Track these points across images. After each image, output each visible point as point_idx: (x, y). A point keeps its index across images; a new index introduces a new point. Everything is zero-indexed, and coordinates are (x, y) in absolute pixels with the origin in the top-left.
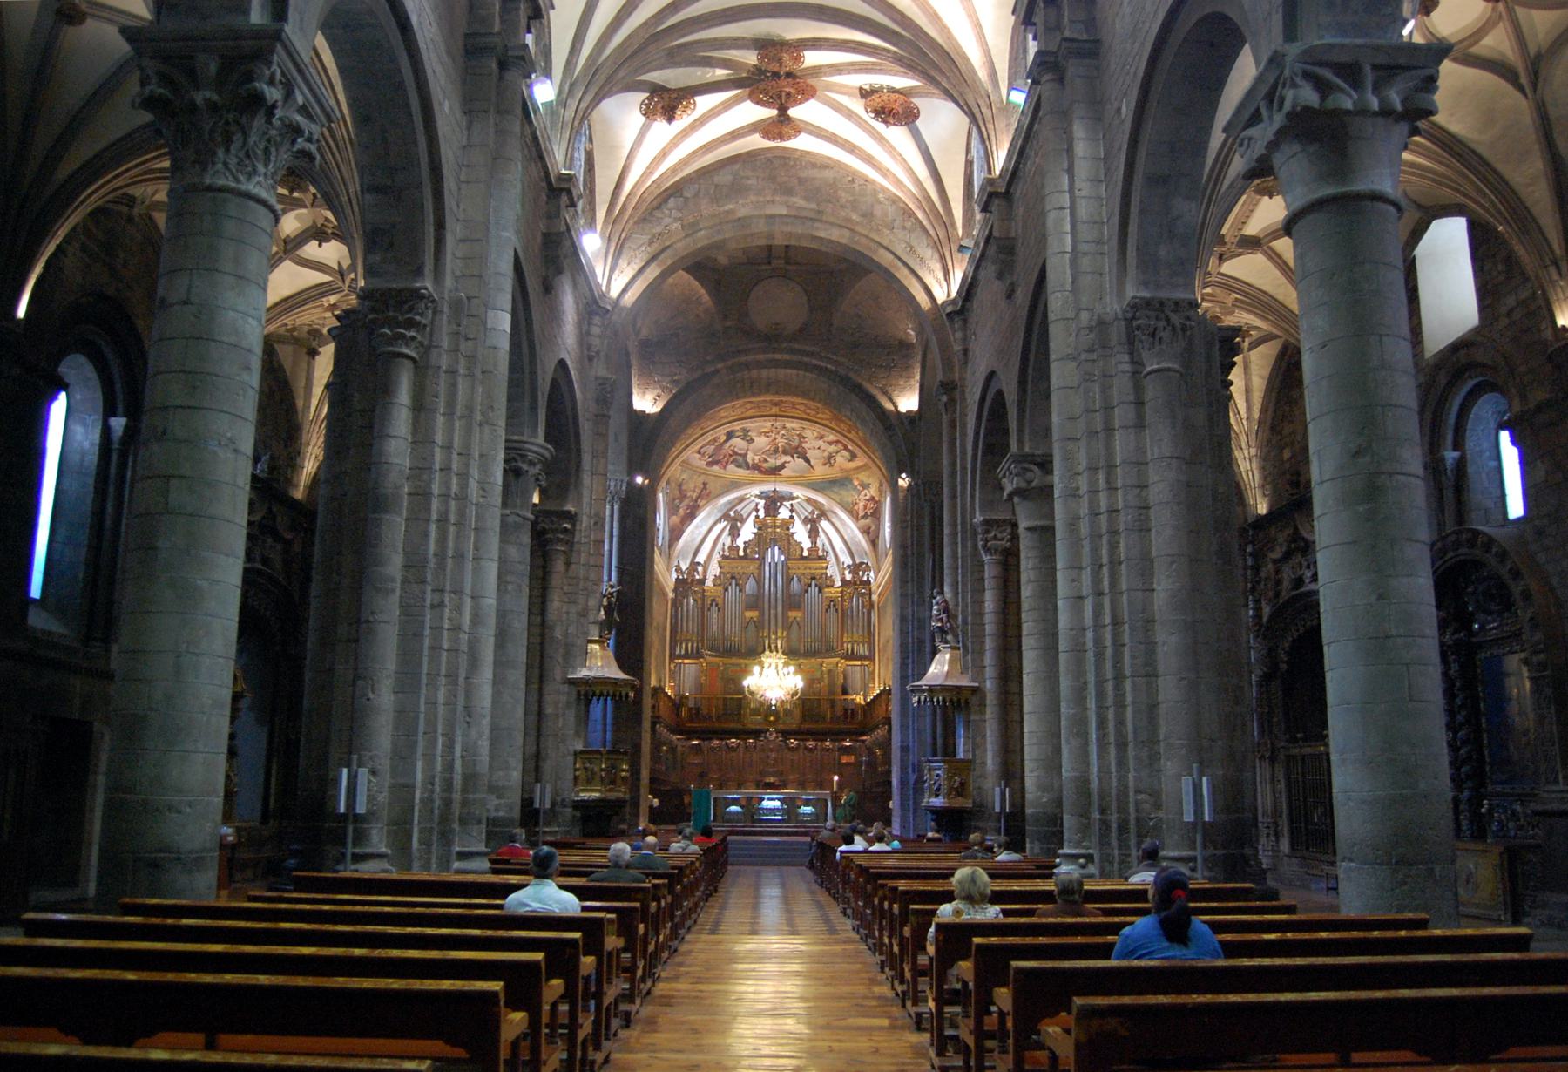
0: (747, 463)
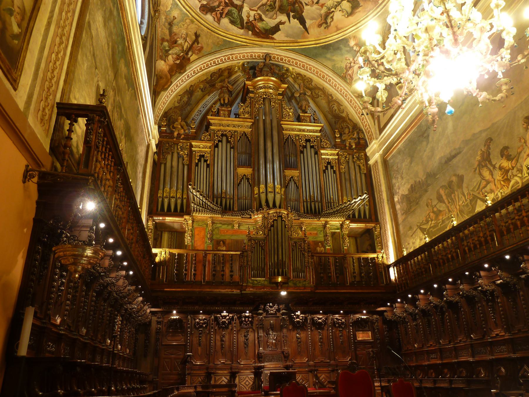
0: (242, 19)
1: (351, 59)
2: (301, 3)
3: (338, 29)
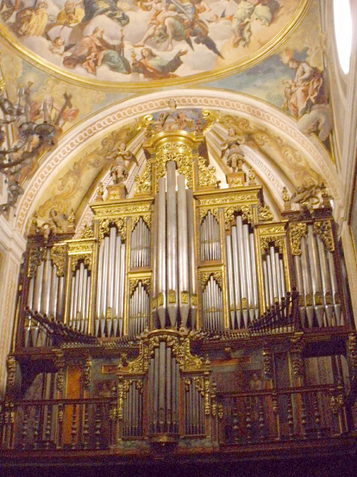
0: (125, 62)
1: (290, 82)
2: (201, 21)
3: (262, 44)
